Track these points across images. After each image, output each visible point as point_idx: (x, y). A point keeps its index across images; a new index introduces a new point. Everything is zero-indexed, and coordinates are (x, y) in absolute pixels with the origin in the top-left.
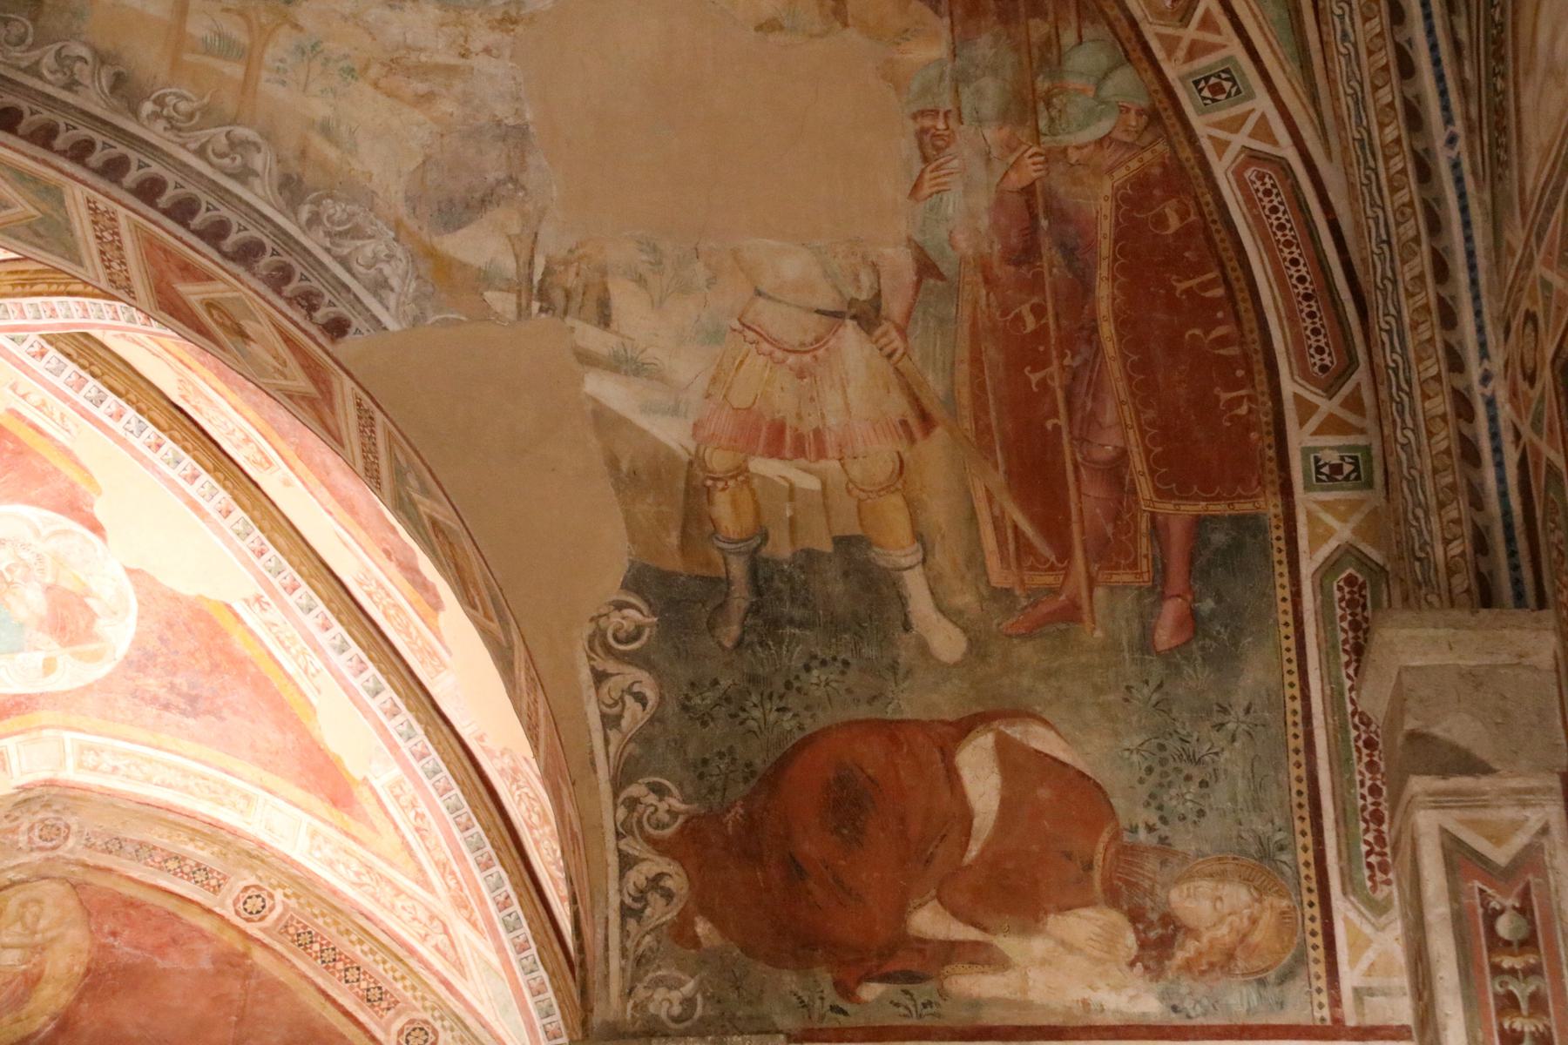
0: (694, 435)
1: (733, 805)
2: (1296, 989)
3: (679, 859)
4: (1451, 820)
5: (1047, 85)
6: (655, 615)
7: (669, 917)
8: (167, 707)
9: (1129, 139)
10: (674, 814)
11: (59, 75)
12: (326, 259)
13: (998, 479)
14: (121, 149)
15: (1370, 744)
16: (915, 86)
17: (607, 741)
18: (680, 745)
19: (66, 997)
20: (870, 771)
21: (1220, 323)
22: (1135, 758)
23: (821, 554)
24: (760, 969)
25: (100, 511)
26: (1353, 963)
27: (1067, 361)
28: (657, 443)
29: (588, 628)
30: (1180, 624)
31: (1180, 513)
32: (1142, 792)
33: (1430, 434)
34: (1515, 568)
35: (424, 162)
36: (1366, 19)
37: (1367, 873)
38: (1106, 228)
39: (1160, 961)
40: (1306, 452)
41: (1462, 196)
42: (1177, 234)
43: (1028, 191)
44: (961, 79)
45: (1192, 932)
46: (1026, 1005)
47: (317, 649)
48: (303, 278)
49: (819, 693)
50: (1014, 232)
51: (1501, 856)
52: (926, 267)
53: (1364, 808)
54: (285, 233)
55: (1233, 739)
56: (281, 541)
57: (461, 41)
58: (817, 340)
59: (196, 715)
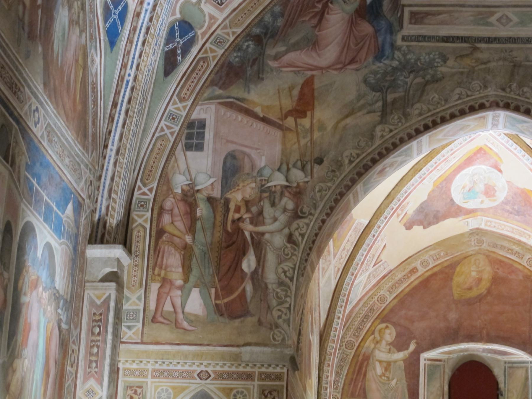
8: (511, 213)
19: (488, 285)
25: (502, 168)
59: (518, 215)
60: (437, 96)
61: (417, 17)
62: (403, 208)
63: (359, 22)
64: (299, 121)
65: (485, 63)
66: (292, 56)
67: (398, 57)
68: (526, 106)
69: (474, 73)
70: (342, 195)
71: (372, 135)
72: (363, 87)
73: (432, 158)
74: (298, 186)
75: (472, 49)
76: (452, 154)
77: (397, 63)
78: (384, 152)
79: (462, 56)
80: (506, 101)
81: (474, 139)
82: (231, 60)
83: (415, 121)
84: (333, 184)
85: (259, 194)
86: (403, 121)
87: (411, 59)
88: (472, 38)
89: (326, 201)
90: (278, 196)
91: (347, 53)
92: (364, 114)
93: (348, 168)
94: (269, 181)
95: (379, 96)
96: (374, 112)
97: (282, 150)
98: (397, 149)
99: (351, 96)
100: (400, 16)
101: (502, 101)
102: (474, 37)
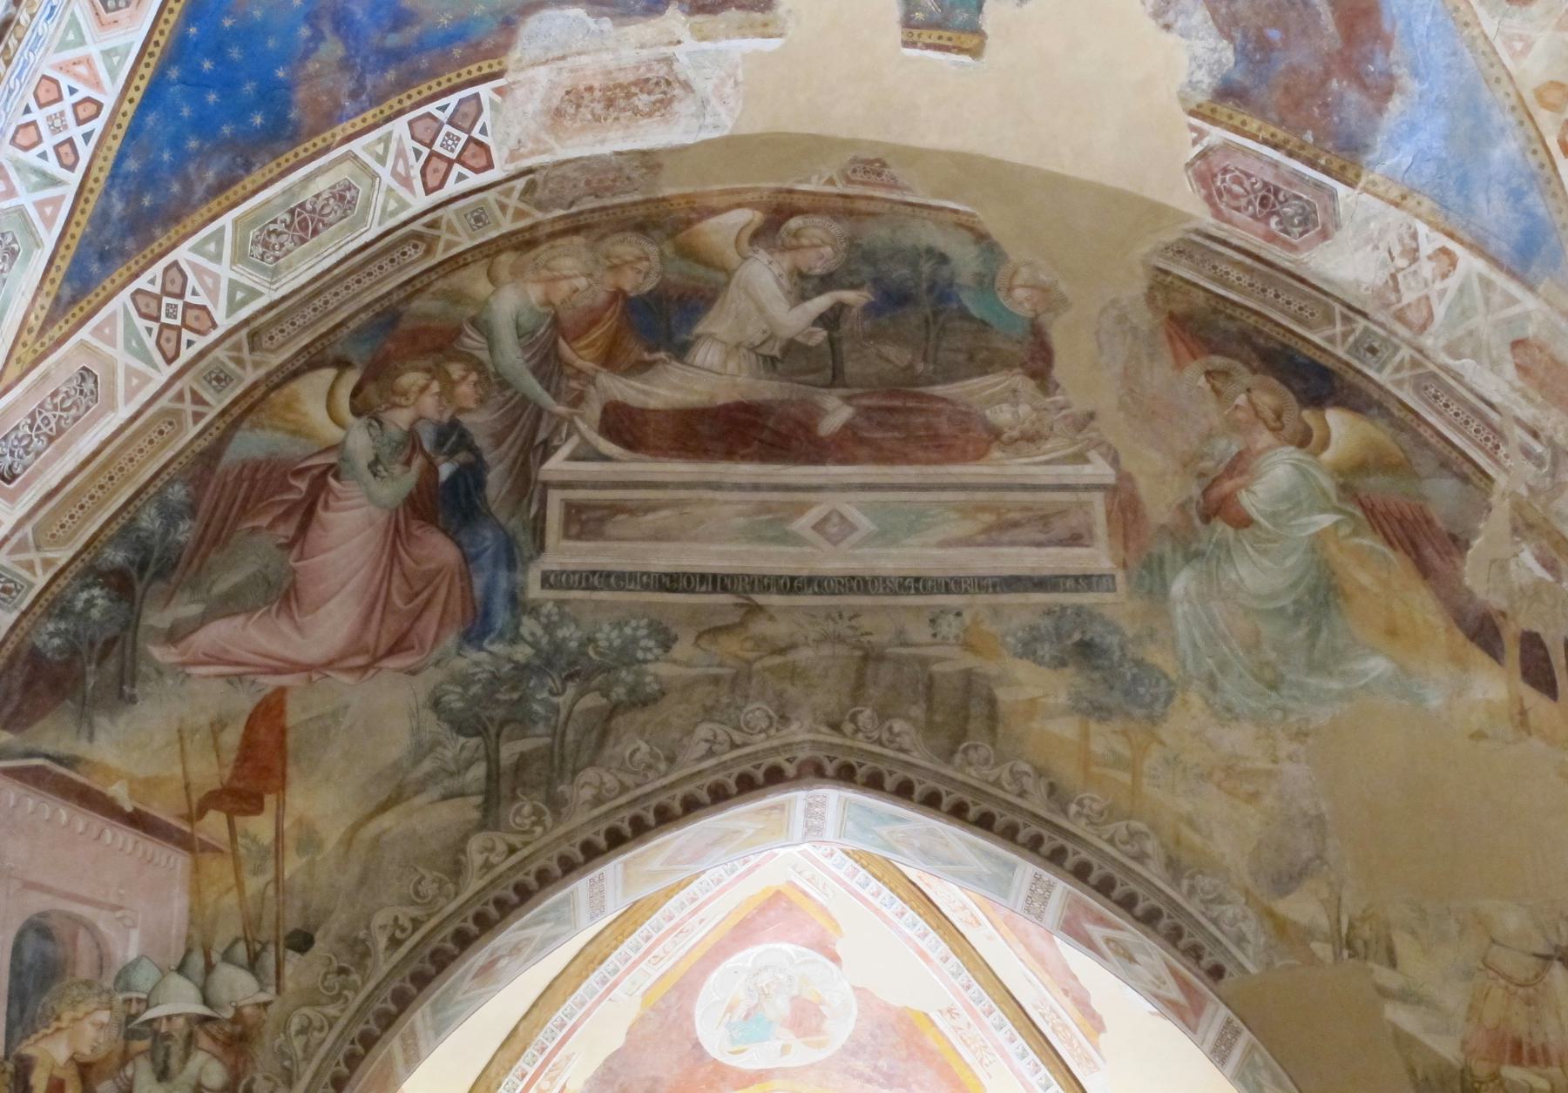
0: (1462, 1050)
8: (869, 1081)
11: (1014, 787)
14: (1060, 841)
47: (1004, 1055)
56: (980, 977)
58: (1536, 976)
60: (644, 747)
61: (584, 517)
62: (553, 1074)
63: (418, 533)
64: (239, 821)
65: (782, 651)
66: (219, 633)
67: (533, 634)
68: (901, 774)
69: (749, 678)
70: (368, 1041)
71: (457, 862)
72: (430, 719)
73: (638, 924)
74: (238, 1017)
75: (743, 611)
76: (694, 912)
77: (529, 651)
78: (492, 911)
79: (715, 631)
80: (842, 759)
81: (757, 866)
82: (39, 644)
83: (582, 821)
84: (343, 1011)
85: (121, 1042)
86: (548, 819)
87: (571, 640)
88: (743, 580)
89: (323, 1060)
90: (177, 1049)
91: (382, 620)
92: (432, 803)
93: (385, 961)
94: (153, 1001)
95: (478, 747)
96: (462, 794)
97: (191, 910)
98: (530, 902)
99: (396, 745)
100: (535, 518)
101: (831, 759)
102: (748, 576)
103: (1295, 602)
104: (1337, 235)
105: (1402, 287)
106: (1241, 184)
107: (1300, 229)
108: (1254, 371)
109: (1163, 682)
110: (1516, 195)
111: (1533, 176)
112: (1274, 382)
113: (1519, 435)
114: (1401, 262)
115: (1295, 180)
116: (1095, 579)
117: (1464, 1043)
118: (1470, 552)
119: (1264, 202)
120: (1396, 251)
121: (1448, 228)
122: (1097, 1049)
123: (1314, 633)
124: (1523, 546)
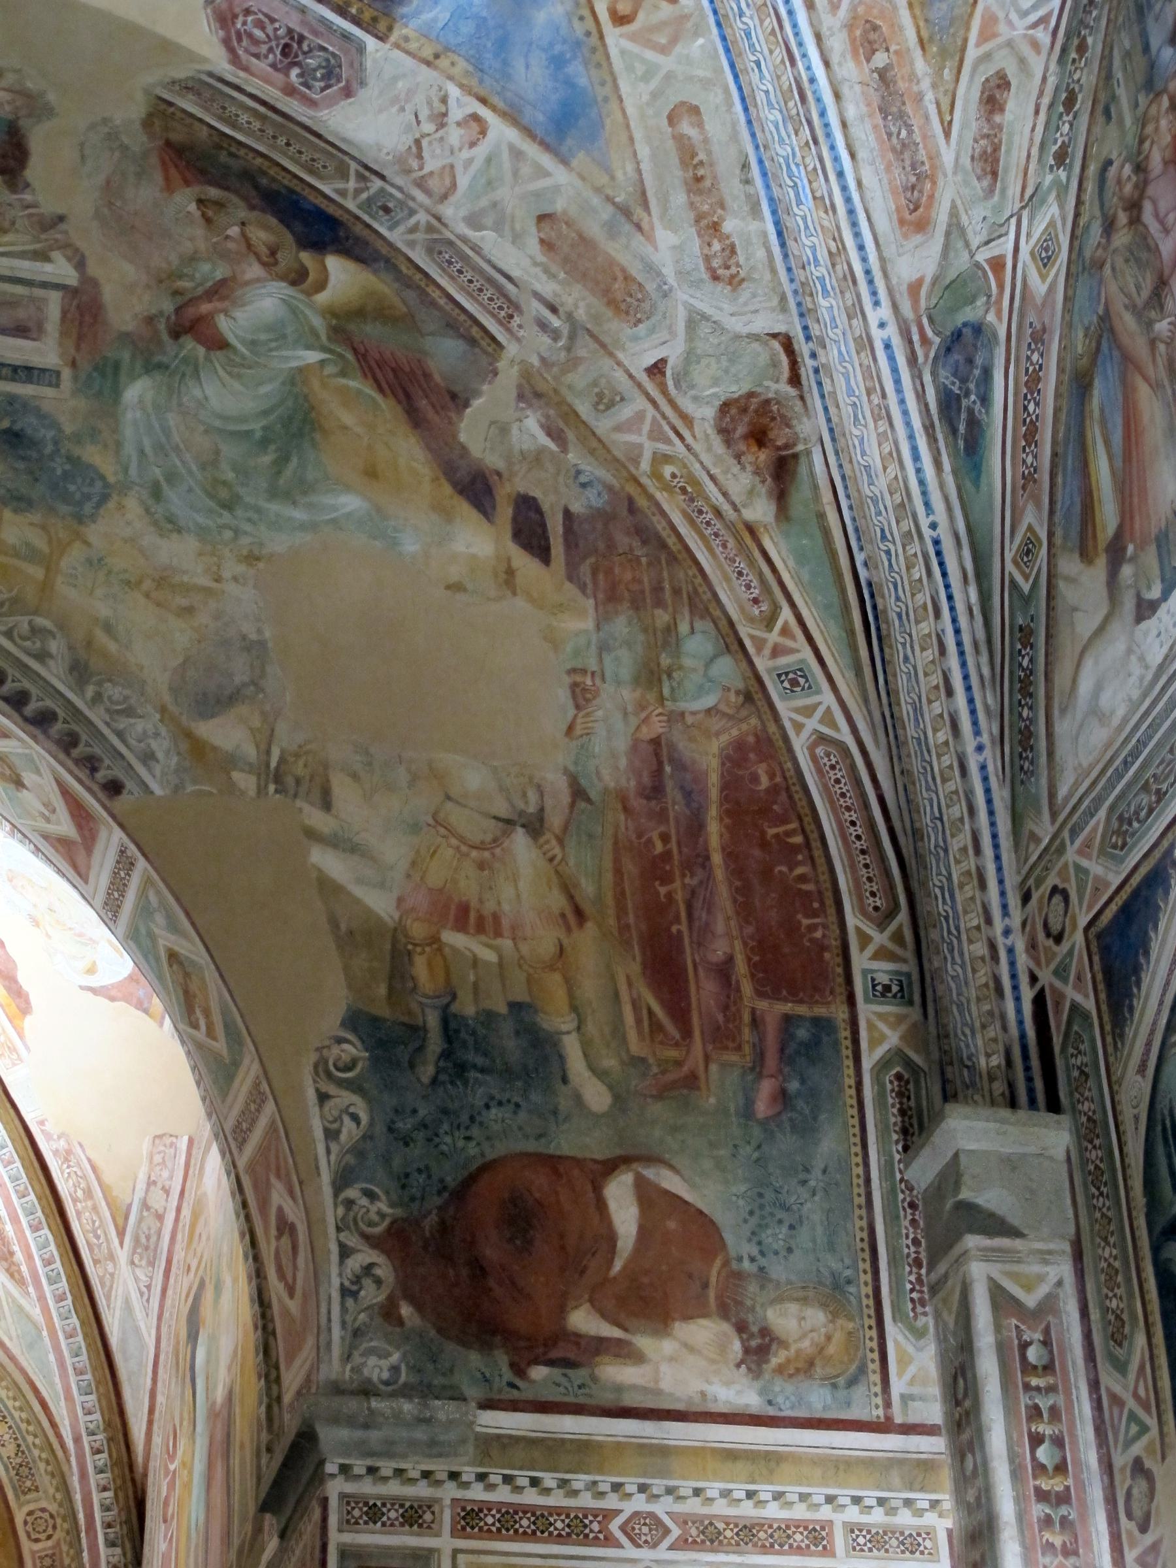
0: (398, 907)
1: (430, 1213)
2: (860, 1391)
3: (387, 1253)
4: (995, 1270)
5: (669, 661)
6: (367, 1050)
7: (379, 1299)
9: (730, 712)
10: (382, 1216)
12: (106, 731)
13: (635, 967)
15: (912, 1205)
16: (569, 648)
17: (328, 1152)
18: (386, 1160)
20: (537, 1195)
21: (798, 864)
22: (741, 1202)
23: (498, 1015)
24: (451, 1348)
26: (900, 1374)
27: (687, 880)
28: (369, 911)
29: (313, 1057)
30: (774, 1099)
31: (774, 1010)
32: (746, 1230)
33: (974, 971)
34: (1029, 1079)
35: (184, 662)
36: (923, 649)
37: (910, 1306)
38: (714, 779)
39: (759, 1364)
40: (865, 972)
41: (988, 791)
42: (767, 791)
43: (656, 742)
44: (603, 648)
45: (783, 1344)
46: (659, 1392)
48: (88, 745)
49: (496, 1127)
50: (645, 774)
51: (1031, 1300)
52: (578, 793)
53: (908, 1255)
54: (74, 707)
55: (814, 1194)
57: (215, 568)
58: (495, 840)
103: (264, 428)
104: (363, 94)
105: (425, 154)
106: (263, 28)
107: (322, 84)
108: (252, 208)
109: (99, 484)
110: (558, 62)
111: (578, 44)
112: (273, 221)
113: (537, 308)
114: (428, 127)
115: (322, 29)
116: (36, 372)
117: (400, 900)
118: (468, 410)
119: (286, 50)
120: (424, 114)
121: (482, 93)
122: (21, 1036)
123: (282, 460)
124: (529, 412)
